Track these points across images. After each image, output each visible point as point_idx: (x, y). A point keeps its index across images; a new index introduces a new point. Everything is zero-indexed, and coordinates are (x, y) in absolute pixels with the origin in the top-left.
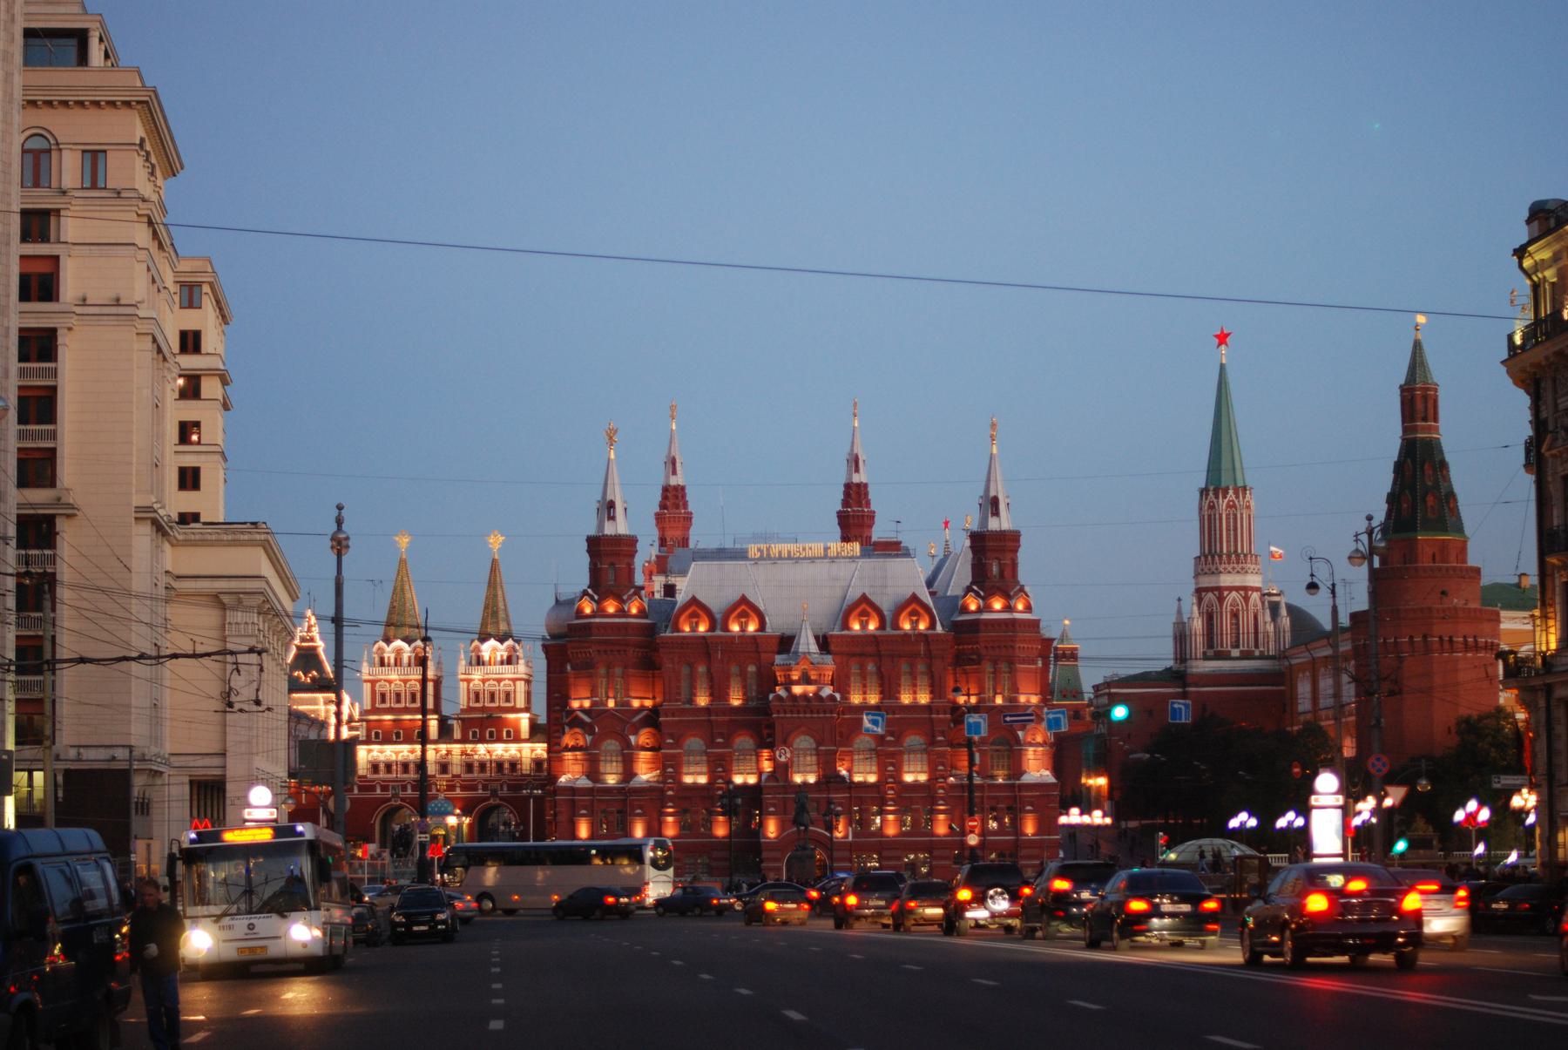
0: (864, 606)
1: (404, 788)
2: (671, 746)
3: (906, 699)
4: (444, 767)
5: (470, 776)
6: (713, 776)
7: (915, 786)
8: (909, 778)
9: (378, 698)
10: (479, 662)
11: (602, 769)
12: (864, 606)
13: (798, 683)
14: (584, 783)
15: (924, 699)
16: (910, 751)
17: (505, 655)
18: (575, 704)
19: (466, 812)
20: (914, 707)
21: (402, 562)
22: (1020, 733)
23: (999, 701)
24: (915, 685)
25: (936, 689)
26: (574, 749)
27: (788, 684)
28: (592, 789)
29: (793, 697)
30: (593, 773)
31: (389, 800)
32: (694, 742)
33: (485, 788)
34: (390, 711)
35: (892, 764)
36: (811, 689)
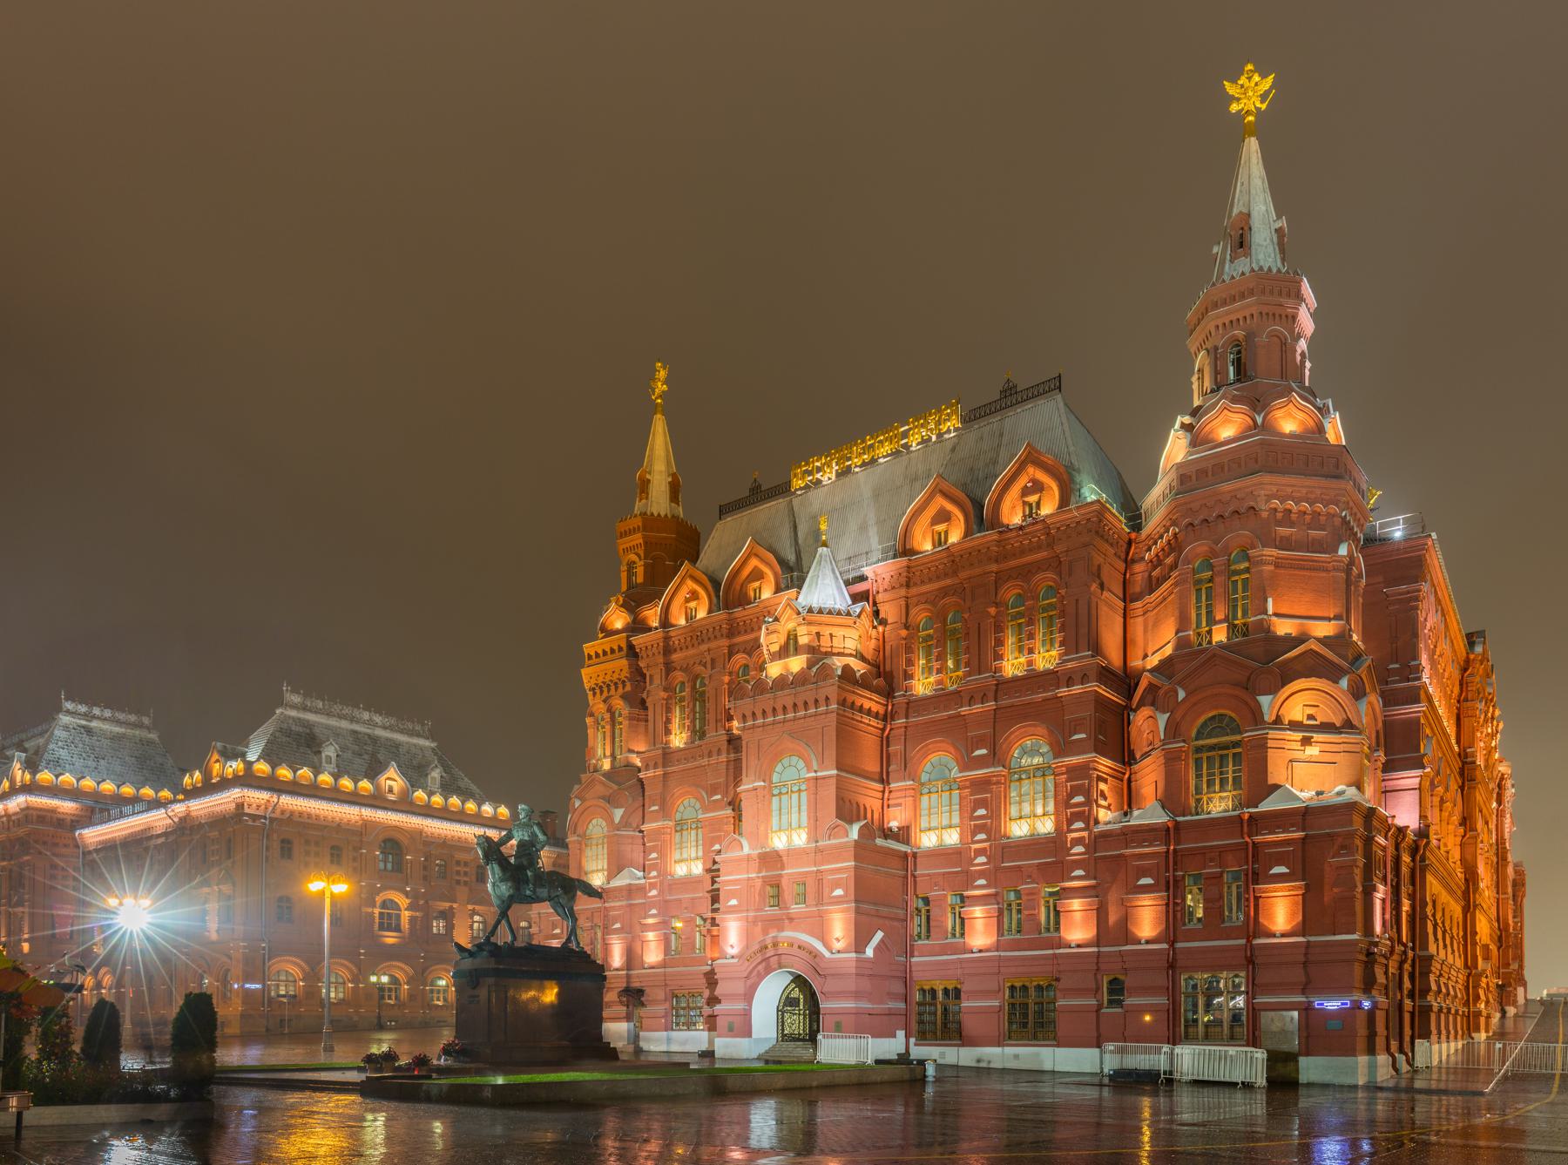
3: (1013, 665)
8: (1019, 830)
15: (1046, 658)
20: (1034, 679)
22: (1265, 700)
23: (1220, 635)
36: (796, 664)
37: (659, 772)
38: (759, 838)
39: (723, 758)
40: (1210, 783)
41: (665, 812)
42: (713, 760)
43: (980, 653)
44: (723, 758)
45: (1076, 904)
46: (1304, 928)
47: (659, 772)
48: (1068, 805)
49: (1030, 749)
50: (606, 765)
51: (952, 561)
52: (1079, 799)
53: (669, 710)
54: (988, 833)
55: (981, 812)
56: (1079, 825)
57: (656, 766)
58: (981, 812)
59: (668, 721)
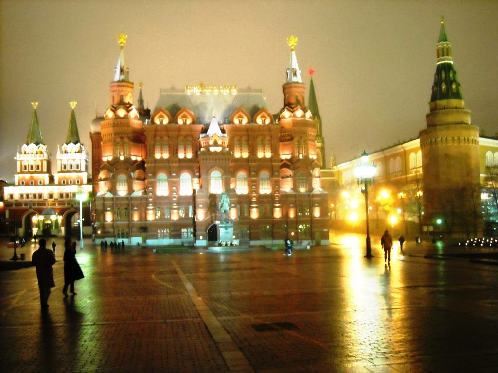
2: (151, 177)
4: (51, 196)
5: (61, 199)
7: (265, 196)
9: (23, 167)
12: (240, 113)
14: (109, 195)
16: (263, 179)
19: (61, 213)
20: (264, 159)
21: (36, 113)
24: (264, 150)
25: (275, 151)
28: (113, 199)
30: (113, 190)
33: (68, 204)
34: (29, 173)
35: (255, 185)
37: (153, 165)
41: (154, 175)
46: (320, 216)
47: (153, 165)
49: (264, 174)
50: (122, 158)
54: (256, 192)
55: (254, 187)
57: (152, 163)
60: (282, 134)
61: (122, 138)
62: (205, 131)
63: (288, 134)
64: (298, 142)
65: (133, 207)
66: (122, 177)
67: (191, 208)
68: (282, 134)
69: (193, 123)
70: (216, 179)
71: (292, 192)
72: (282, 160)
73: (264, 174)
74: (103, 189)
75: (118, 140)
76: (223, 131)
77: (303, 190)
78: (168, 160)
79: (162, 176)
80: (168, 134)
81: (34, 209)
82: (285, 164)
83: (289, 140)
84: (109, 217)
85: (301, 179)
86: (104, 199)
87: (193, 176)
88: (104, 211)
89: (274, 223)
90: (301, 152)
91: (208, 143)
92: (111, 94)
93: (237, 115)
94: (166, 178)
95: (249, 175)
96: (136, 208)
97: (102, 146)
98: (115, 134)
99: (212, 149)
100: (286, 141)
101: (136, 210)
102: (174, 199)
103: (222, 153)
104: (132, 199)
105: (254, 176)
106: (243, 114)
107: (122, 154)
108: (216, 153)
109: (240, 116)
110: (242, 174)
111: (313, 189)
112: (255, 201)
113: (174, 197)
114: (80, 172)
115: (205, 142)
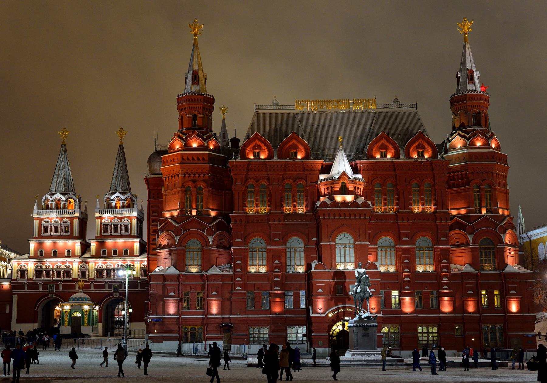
0: (383, 141)
1: (57, 287)
2: (238, 244)
3: (417, 209)
6: (271, 267)
8: (420, 269)
9: (43, 229)
10: (109, 206)
11: (187, 262)
12: (383, 141)
13: (339, 193)
14: (173, 271)
17: (126, 202)
18: (168, 215)
20: (423, 215)
26: (165, 247)
27: (331, 195)
29: (336, 204)
31: (48, 295)
32: (258, 242)
35: (408, 258)
38: (333, 264)
39: (282, 223)
40: (486, 260)
41: (245, 240)
42: (277, 223)
43: (404, 202)
44: (282, 223)
45: (446, 298)
48: (441, 263)
51: (392, 165)
52: (444, 261)
53: (245, 195)
55: (406, 261)
56: (445, 270)
58: (406, 261)
59: (245, 201)
60: (452, 174)
61: (194, 181)
62: (327, 169)
63: (462, 174)
64: (479, 187)
65: (210, 291)
66: (194, 243)
67: (303, 294)
68: (452, 174)
69: (307, 157)
70: (345, 248)
71: (472, 270)
72: (452, 217)
73: (424, 240)
74: (164, 265)
75: (190, 184)
76: (355, 170)
77: (488, 268)
78: (267, 216)
79: (258, 242)
80: (268, 175)
81: (56, 294)
82: (459, 224)
83: (463, 185)
84: (172, 309)
85: (485, 249)
86: (163, 277)
87: (307, 241)
88: (163, 298)
89: (443, 323)
90: (483, 205)
91: (332, 188)
92: (177, 113)
93: (377, 146)
94: (264, 245)
95: (398, 240)
96: (214, 293)
97: (164, 194)
98: (185, 175)
99: (339, 198)
100: (458, 186)
101: (214, 296)
102: (277, 279)
103: (354, 204)
104: (209, 278)
105: (406, 243)
106: (387, 144)
107: (194, 206)
108: (344, 203)
109: (384, 147)
110: (386, 240)
111: (507, 264)
112: (408, 285)
113: (276, 276)
114: (130, 236)
115: (326, 187)
